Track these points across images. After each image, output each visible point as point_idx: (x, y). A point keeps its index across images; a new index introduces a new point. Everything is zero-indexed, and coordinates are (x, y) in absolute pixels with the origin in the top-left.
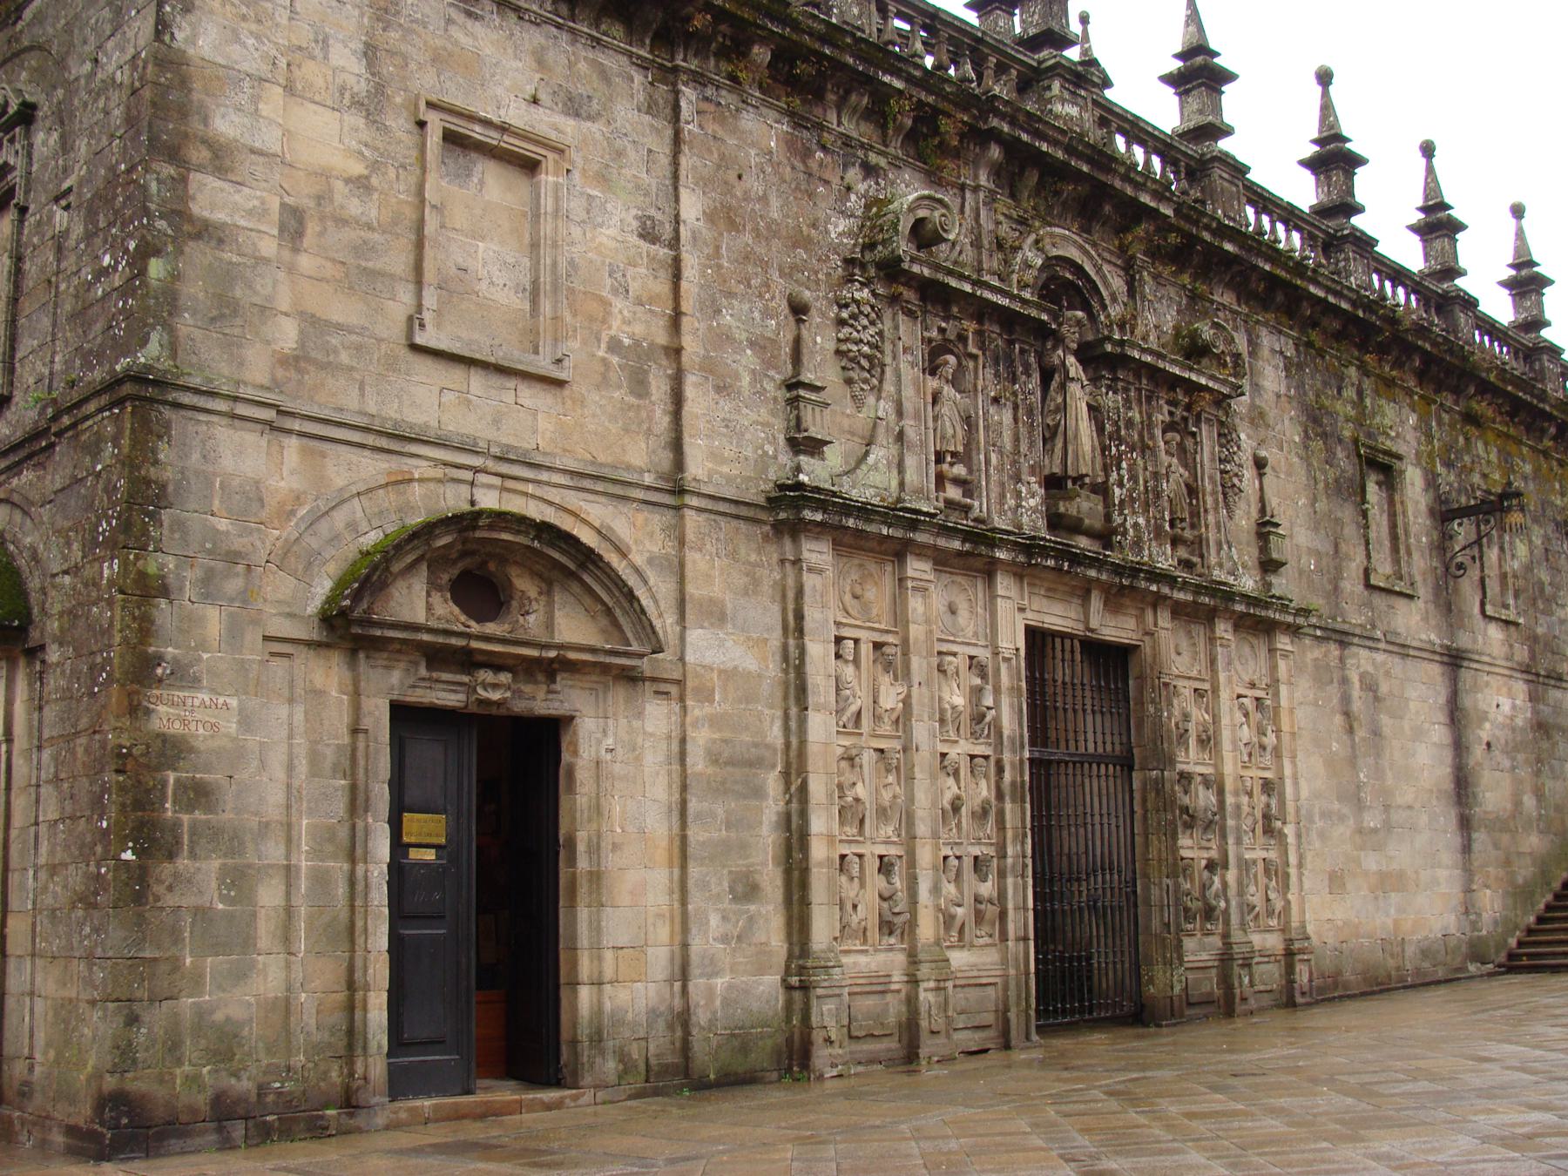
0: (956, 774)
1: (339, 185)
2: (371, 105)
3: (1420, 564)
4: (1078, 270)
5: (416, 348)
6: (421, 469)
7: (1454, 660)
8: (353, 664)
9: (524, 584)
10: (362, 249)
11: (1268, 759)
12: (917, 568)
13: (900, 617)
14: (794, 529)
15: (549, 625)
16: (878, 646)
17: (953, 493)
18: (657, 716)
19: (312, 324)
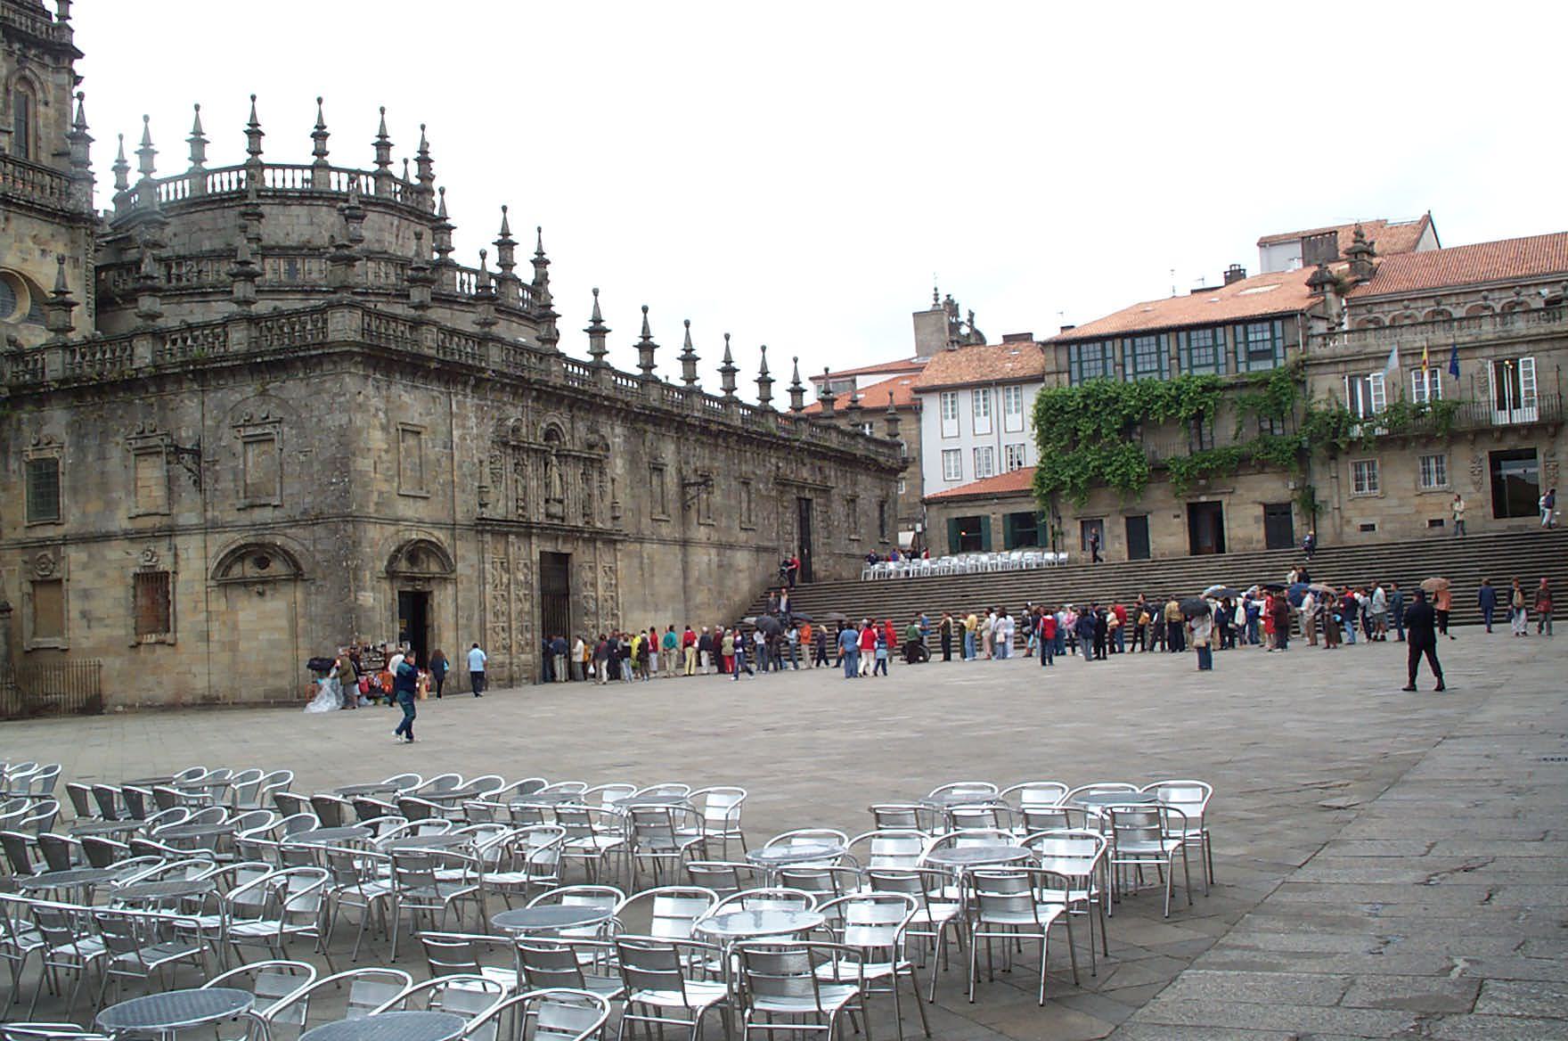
0: (520, 600)
1: (383, 454)
2: (384, 428)
3: (673, 507)
4: (558, 426)
5: (399, 495)
6: (401, 528)
7: (685, 543)
8: (391, 582)
9: (423, 556)
10: (388, 469)
11: (613, 588)
12: (512, 538)
13: (507, 554)
14: (482, 532)
15: (428, 567)
16: (502, 563)
17: (520, 511)
18: (450, 589)
19: (381, 493)
